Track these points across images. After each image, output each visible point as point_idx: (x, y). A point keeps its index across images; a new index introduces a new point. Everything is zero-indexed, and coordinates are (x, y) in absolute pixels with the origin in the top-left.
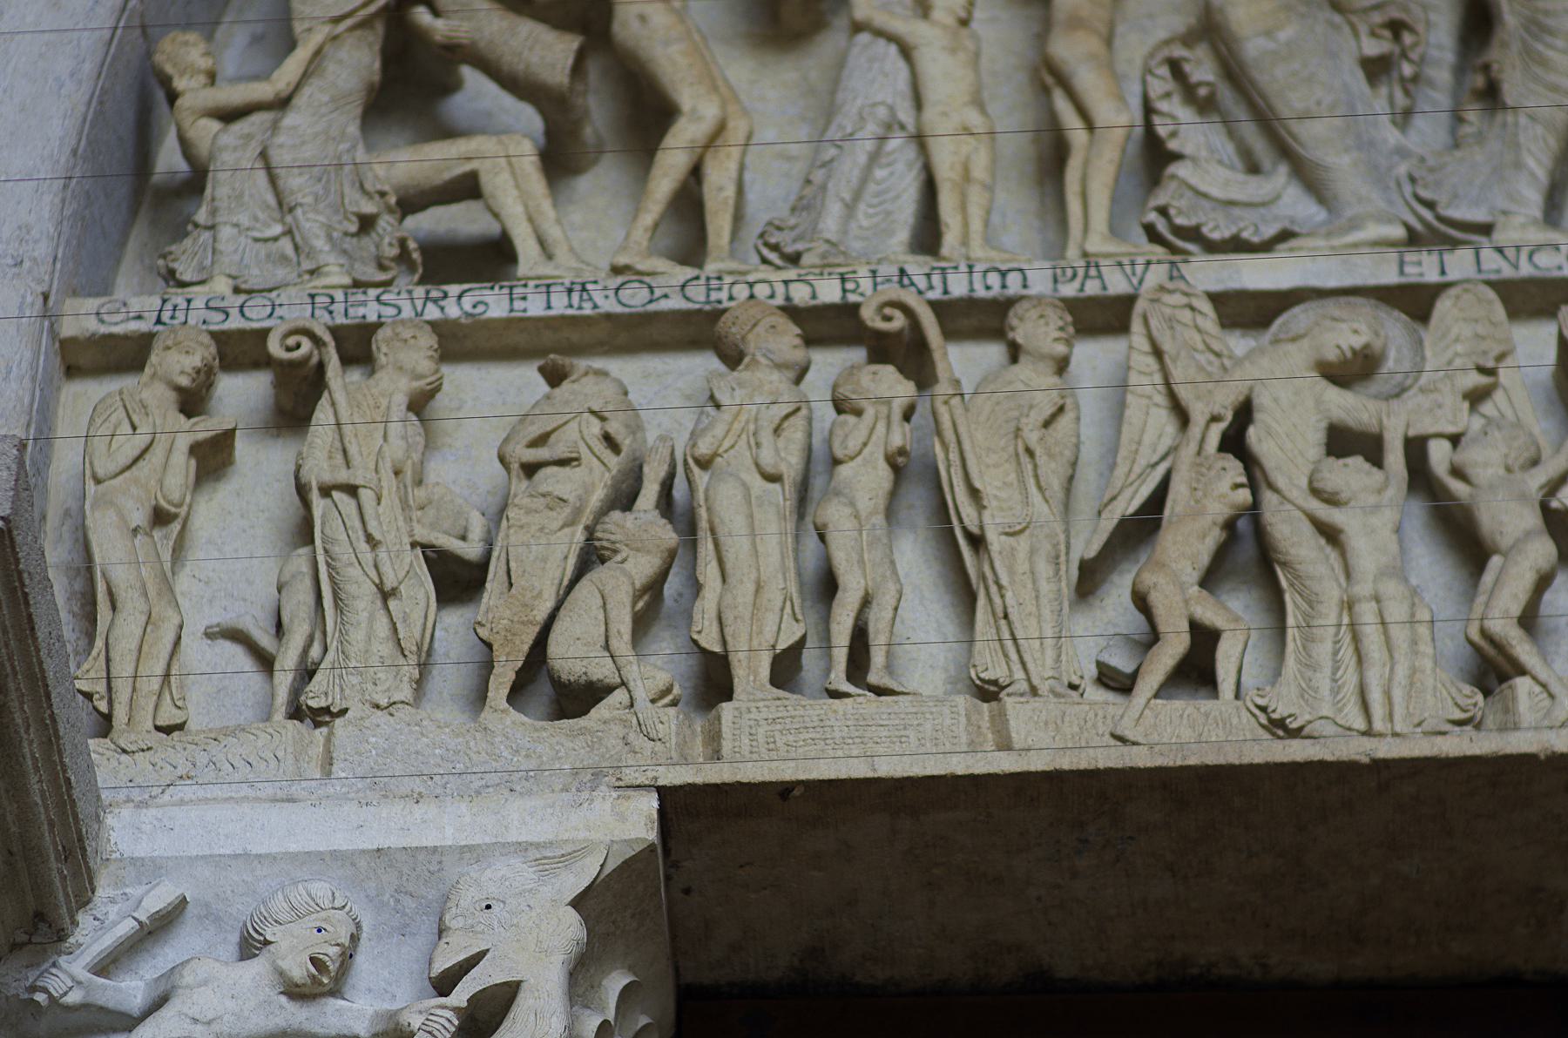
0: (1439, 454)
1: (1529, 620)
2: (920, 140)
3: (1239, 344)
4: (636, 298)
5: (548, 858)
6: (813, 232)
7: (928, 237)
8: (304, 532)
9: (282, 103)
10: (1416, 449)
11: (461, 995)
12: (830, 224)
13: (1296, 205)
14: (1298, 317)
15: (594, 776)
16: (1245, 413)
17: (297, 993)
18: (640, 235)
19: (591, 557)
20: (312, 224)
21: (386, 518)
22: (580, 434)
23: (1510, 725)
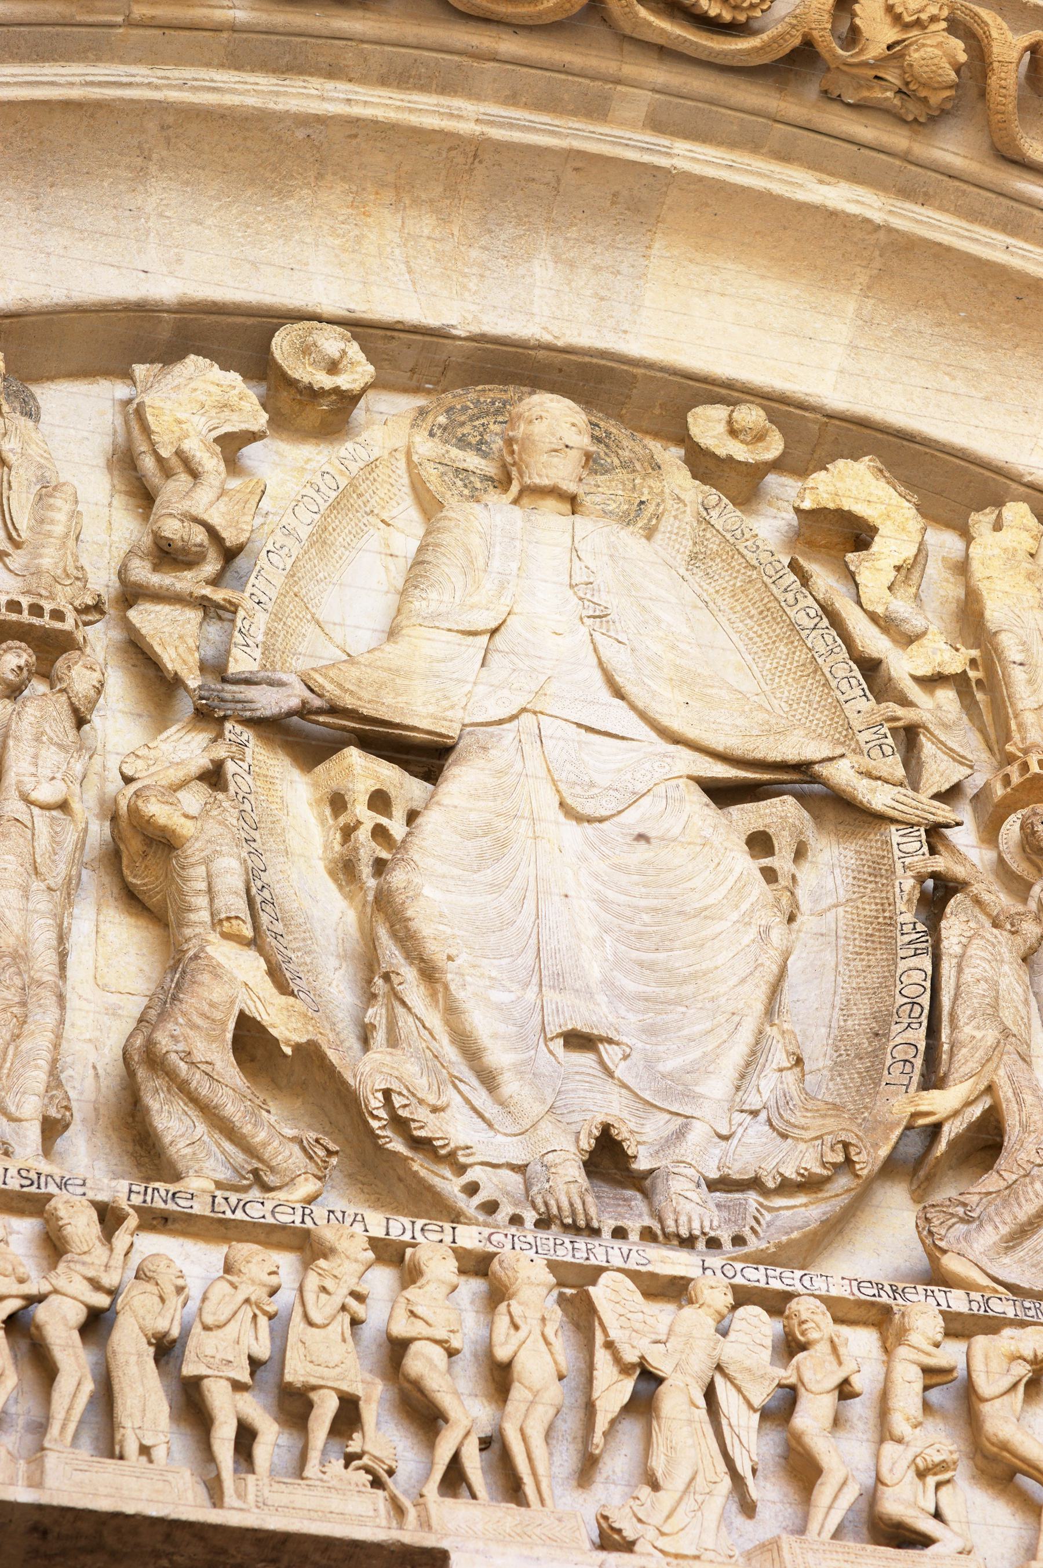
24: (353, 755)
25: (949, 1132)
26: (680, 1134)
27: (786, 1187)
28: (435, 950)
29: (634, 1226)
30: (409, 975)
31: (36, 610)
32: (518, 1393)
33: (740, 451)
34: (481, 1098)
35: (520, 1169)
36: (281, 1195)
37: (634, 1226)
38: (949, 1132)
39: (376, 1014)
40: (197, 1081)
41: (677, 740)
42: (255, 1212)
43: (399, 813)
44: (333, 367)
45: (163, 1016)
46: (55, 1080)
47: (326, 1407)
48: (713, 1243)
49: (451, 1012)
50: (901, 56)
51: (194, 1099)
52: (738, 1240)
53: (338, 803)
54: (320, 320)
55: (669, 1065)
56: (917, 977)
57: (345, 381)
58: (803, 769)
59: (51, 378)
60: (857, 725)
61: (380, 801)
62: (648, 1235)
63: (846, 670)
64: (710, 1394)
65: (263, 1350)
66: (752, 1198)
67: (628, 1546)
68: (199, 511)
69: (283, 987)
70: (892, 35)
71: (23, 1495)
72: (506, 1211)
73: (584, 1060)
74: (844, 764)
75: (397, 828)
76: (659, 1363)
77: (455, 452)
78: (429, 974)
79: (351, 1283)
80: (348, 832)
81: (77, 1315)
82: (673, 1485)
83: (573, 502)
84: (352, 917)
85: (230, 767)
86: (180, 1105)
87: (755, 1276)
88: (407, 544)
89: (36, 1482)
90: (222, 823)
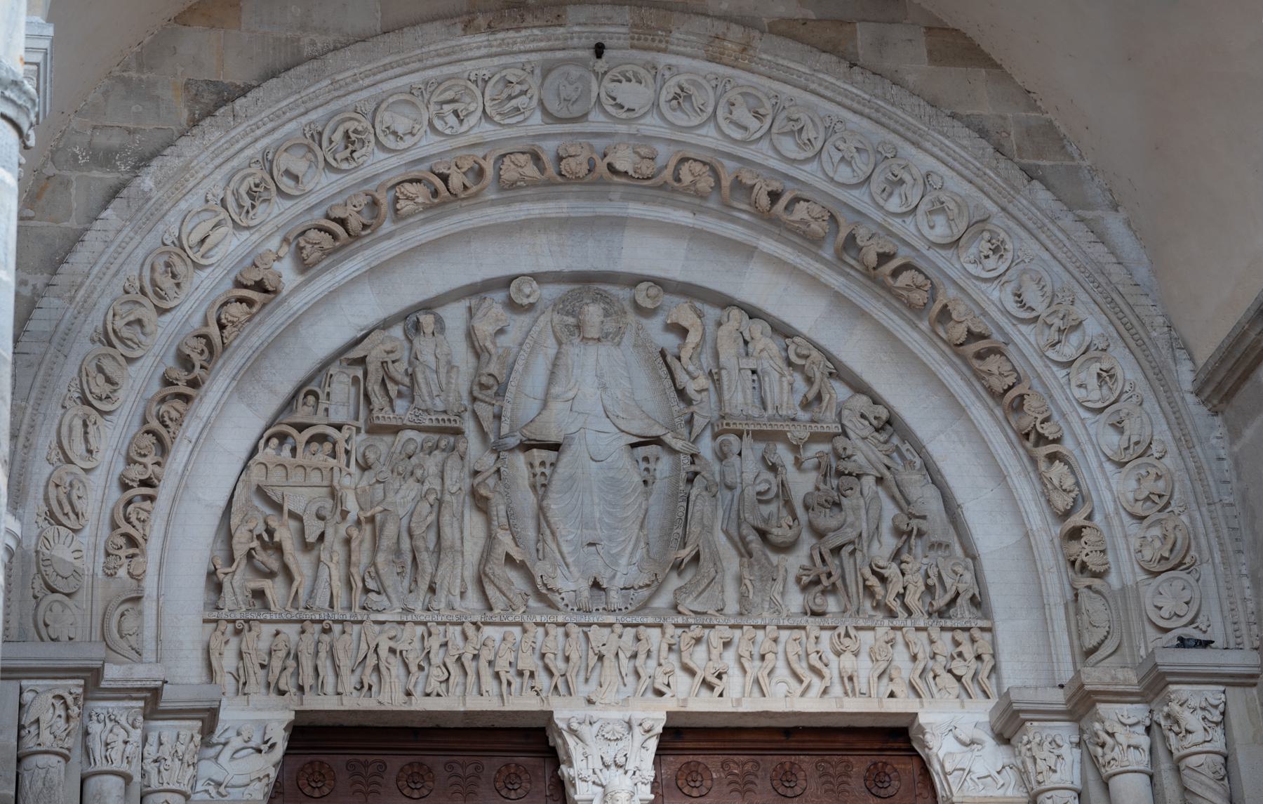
0: (404, 653)
1: (415, 686)
2: (330, 585)
3: (377, 628)
4: (289, 616)
5: (278, 720)
6: (313, 603)
7: (331, 606)
8: (242, 658)
9: (234, 572)
10: (401, 652)
11: (269, 744)
12: (317, 603)
13: (386, 603)
14: (387, 626)
15: (286, 708)
16: (377, 646)
17: (246, 742)
18: (289, 604)
19: (284, 669)
20: (240, 598)
21: (254, 657)
22: (282, 645)
23: (411, 704)
24: (535, 450)
25: (685, 561)
26: (614, 577)
27: (640, 587)
28: (553, 526)
29: (600, 608)
30: (548, 532)
31: (449, 420)
32: (571, 664)
33: (648, 304)
34: (566, 572)
35: (575, 591)
36: (516, 613)
37: (600, 608)
38: (685, 561)
39: (540, 545)
40: (496, 581)
41: (623, 431)
42: (510, 619)
43: (548, 465)
44: (528, 296)
45: (487, 561)
46: (463, 580)
47: (527, 674)
48: (620, 610)
49: (558, 545)
50: (695, 184)
51: (495, 585)
52: (626, 608)
53: (532, 465)
54: (524, 275)
55: (613, 551)
56: (682, 509)
57: (531, 300)
58: (658, 437)
59: (447, 303)
60: (675, 416)
61: (543, 464)
62: (604, 609)
63: (673, 394)
64: (617, 654)
65: (512, 660)
66: (632, 591)
67: (594, 703)
68: (491, 371)
69: (517, 546)
70: (691, 178)
71: (462, 709)
72: (570, 607)
73: (593, 549)
74: (669, 435)
75: (548, 471)
76: (604, 652)
77: (565, 318)
78: (553, 533)
79: (532, 639)
80: (535, 475)
81: (470, 656)
82: (605, 687)
83: (599, 340)
84: (535, 501)
85: (502, 469)
86: (492, 586)
87: (629, 620)
88: (552, 352)
89: (464, 704)
90: (500, 493)
